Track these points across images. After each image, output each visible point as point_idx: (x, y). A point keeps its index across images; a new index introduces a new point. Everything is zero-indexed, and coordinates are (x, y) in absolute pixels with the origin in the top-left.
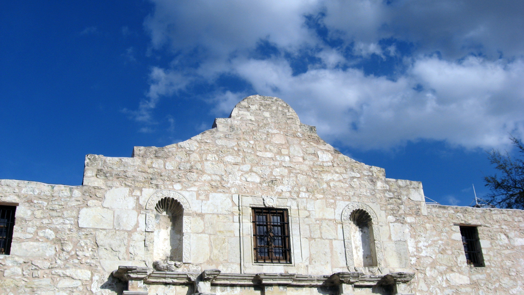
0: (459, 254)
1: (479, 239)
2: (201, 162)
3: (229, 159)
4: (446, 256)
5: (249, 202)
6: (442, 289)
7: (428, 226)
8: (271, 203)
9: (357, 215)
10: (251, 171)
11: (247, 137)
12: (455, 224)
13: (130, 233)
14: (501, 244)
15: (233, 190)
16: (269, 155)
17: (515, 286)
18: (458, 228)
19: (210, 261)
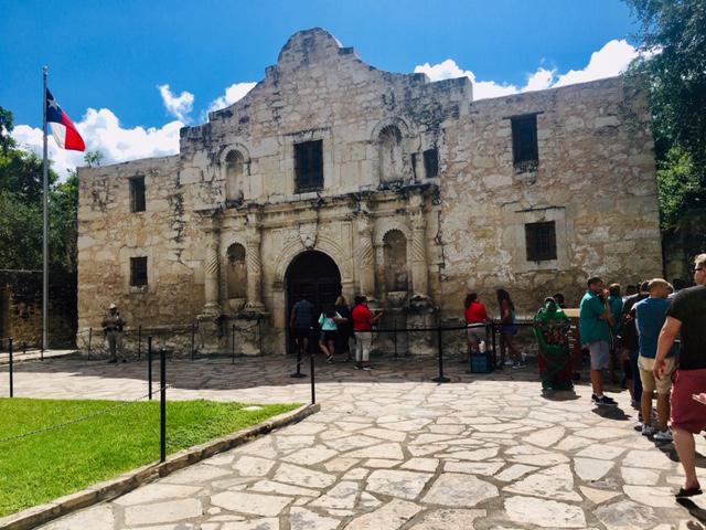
0: (504, 152)
1: (536, 130)
2: (255, 113)
3: (276, 104)
4: (485, 158)
5: (290, 140)
6: (474, 192)
7: (467, 127)
8: (307, 137)
9: (394, 130)
10: (293, 111)
11: (290, 80)
12: (504, 119)
13: (210, 183)
14: (570, 129)
15: (279, 133)
16: (308, 91)
17: (579, 180)
18: (509, 122)
19: (261, 196)
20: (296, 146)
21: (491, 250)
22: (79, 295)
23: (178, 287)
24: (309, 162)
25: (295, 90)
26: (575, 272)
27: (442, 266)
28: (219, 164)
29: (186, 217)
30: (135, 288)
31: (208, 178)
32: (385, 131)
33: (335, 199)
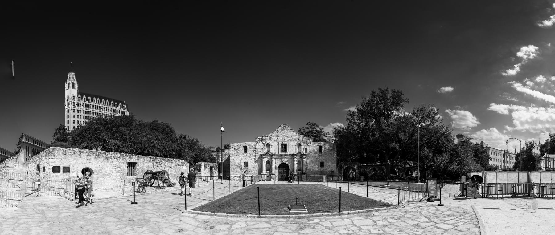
5: (280, 143)
8: (284, 143)
20: (281, 144)
21: (315, 165)
22: (231, 168)
23: (255, 168)
24: (284, 147)
25: (282, 134)
26: (326, 169)
27: (307, 167)
28: (265, 145)
29: (257, 155)
30: (245, 168)
31: (262, 147)
32: (298, 144)
33: (289, 154)
